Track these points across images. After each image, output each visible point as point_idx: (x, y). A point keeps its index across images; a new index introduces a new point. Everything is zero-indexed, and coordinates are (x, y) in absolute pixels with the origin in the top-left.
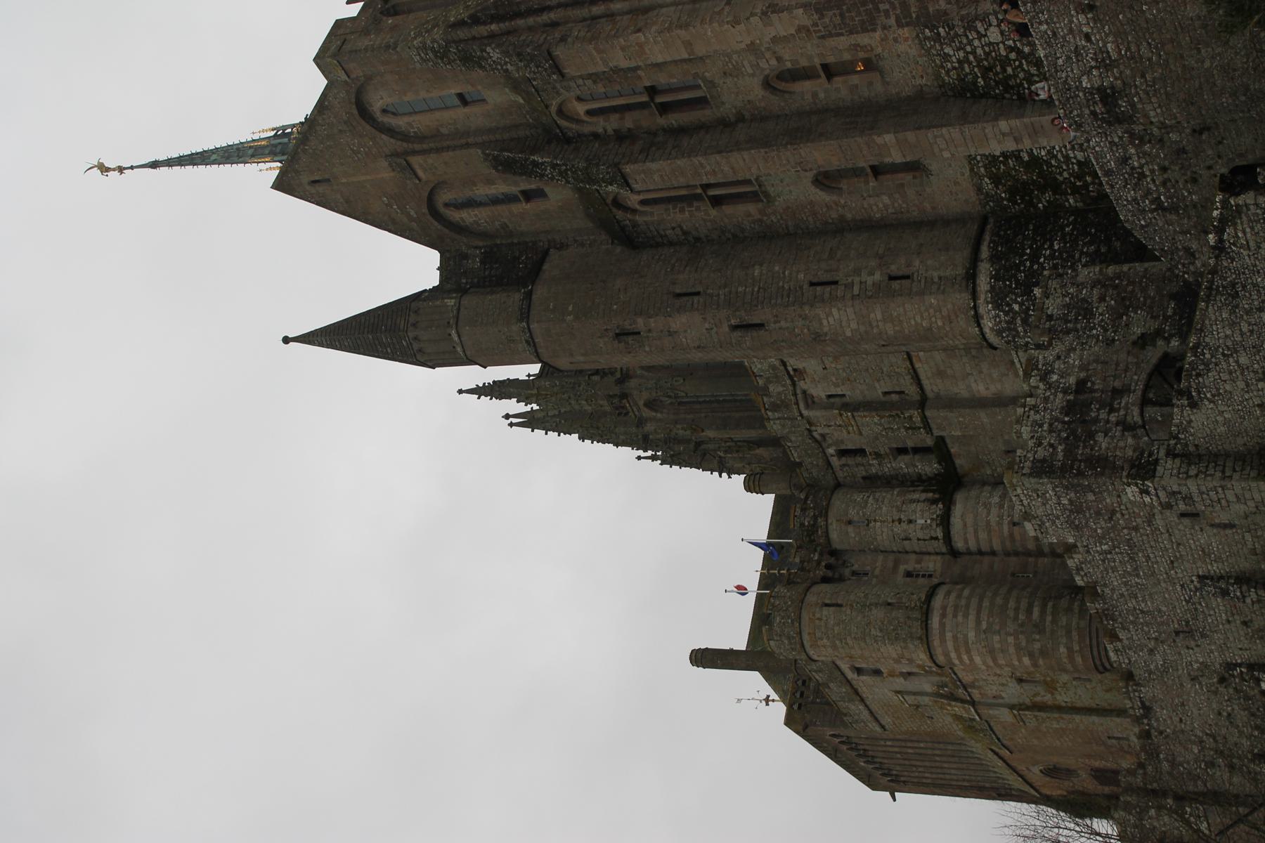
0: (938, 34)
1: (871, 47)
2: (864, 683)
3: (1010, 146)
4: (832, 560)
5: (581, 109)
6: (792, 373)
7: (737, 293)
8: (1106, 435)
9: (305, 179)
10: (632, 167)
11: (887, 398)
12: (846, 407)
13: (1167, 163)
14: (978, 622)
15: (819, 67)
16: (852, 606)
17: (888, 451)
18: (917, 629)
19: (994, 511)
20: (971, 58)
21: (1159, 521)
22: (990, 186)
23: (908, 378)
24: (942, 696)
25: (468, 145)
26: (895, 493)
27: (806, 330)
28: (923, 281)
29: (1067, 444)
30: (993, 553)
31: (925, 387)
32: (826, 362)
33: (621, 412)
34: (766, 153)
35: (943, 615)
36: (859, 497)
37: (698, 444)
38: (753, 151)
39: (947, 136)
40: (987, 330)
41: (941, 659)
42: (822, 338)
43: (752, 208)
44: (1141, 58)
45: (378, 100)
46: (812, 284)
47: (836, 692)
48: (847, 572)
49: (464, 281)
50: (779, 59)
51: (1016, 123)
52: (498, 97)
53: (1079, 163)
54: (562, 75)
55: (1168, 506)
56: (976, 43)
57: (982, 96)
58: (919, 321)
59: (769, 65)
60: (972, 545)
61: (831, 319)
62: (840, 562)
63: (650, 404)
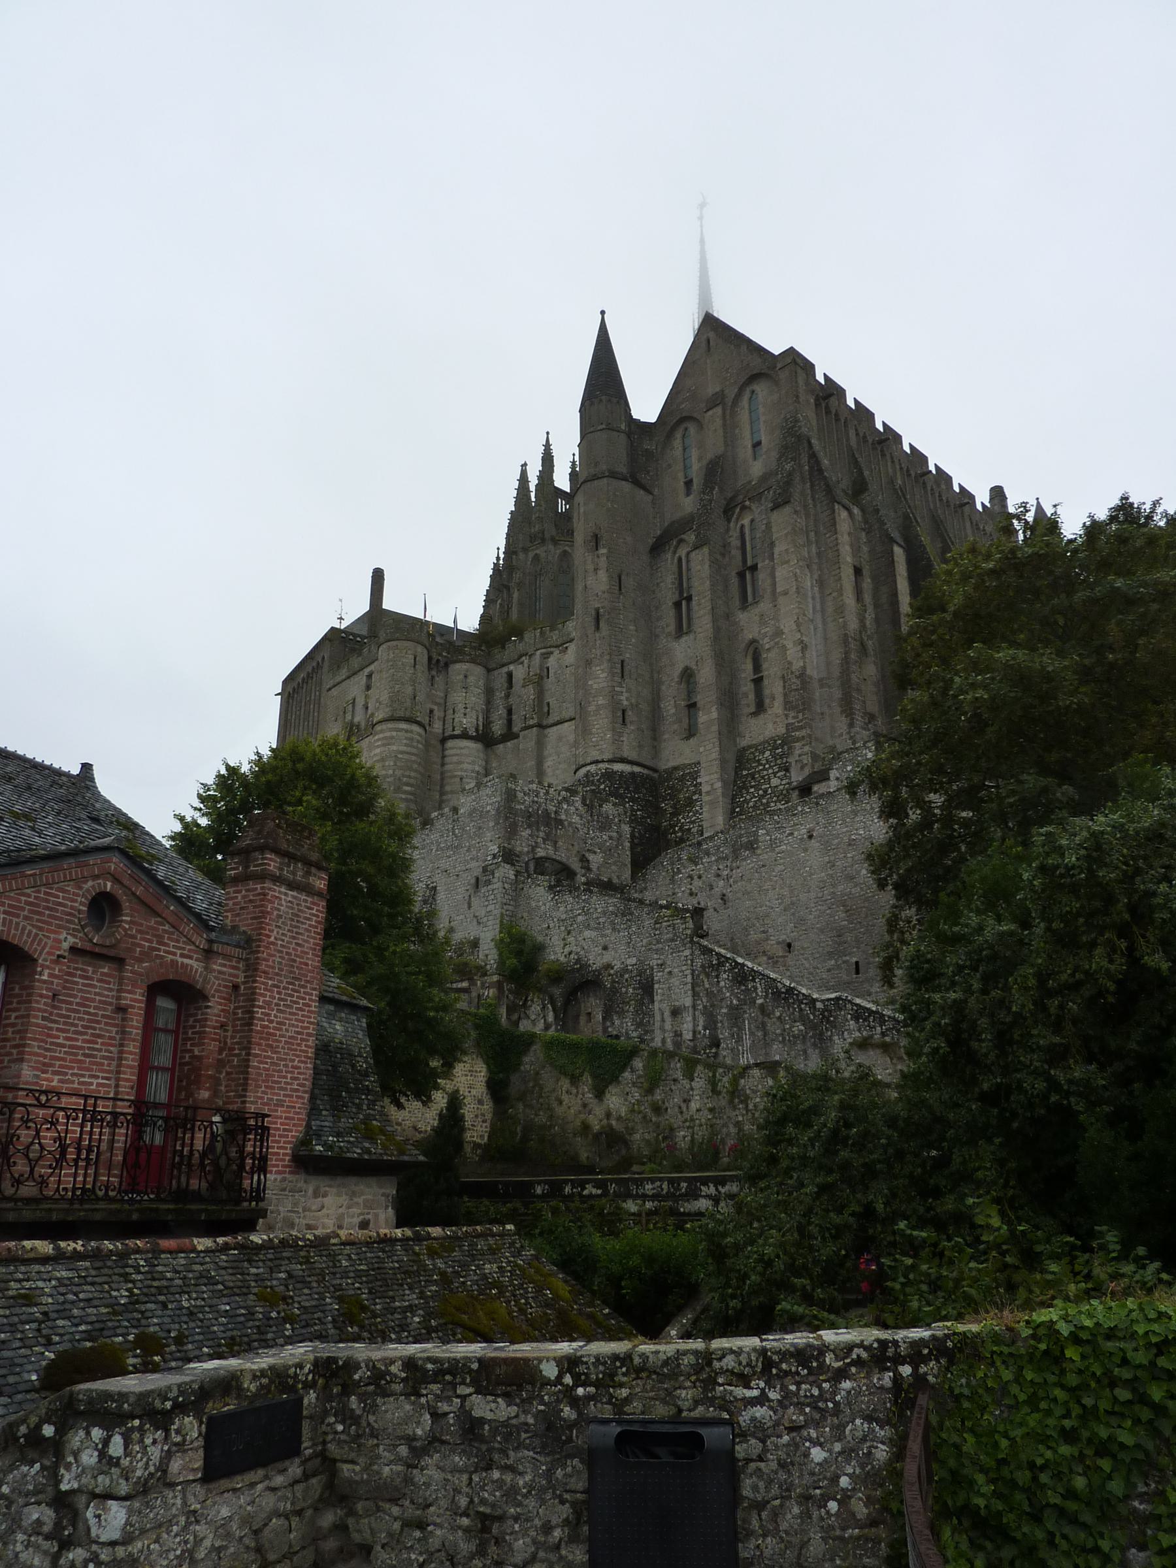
2: (361, 679)
3: (705, 788)
4: (442, 664)
5: (746, 521)
12: (541, 678)
13: (704, 878)
14: (402, 752)
18: (401, 714)
19: (470, 767)
21: (474, 864)
23: (557, 719)
24: (351, 728)
25: (726, 444)
30: (443, 765)
33: (532, 538)
35: (407, 731)
36: (481, 683)
37: (508, 588)
40: (588, 768)
41: (378, 728)
43: (672, 628)
45: (761, 390)
46: (622, 662)
47: (355, 662)
48: (434, 673)
51: (720, 791)
52: (757, 469)
53: (689, 829)
54: (772, 510)
55: (485, 870)
57: (736, 773)
59: (766, 643)
60: (447, 753)
63: (536, 557)
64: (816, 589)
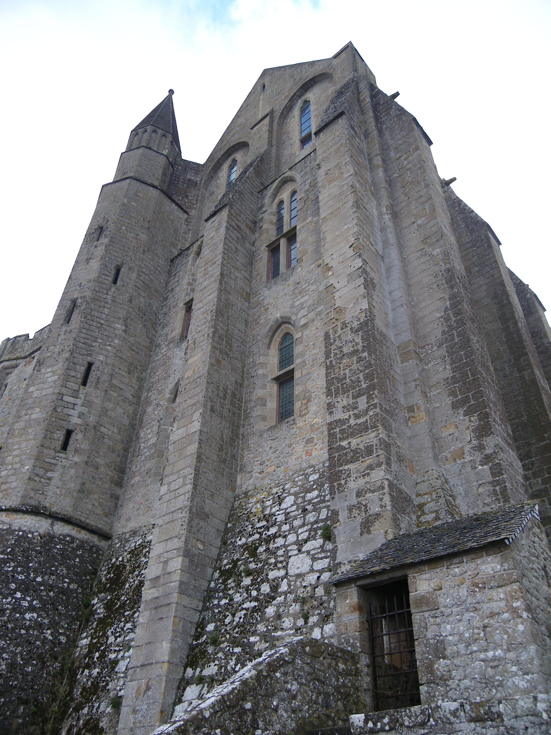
0: (310, 491)
1: (305, 414)
5: (285, 195)
6: (33, 355)
7: (104, 307)
9: (267, 81)
10: (226, 214)
15: (291, 367)
20: (273, 530)
22: (133, 545)
25: (270, 144)
27: (49, 354)
28: (53, 461)
34: (212, 311)
38: (216, 300)
39: (182, 491)
42: (37, 368)
43: (178, 331)
46: (90, 365)
49: (180, 168)
50: (305, 326)
56: (292, 538)
58: (14, 453)
64: (387, 217)
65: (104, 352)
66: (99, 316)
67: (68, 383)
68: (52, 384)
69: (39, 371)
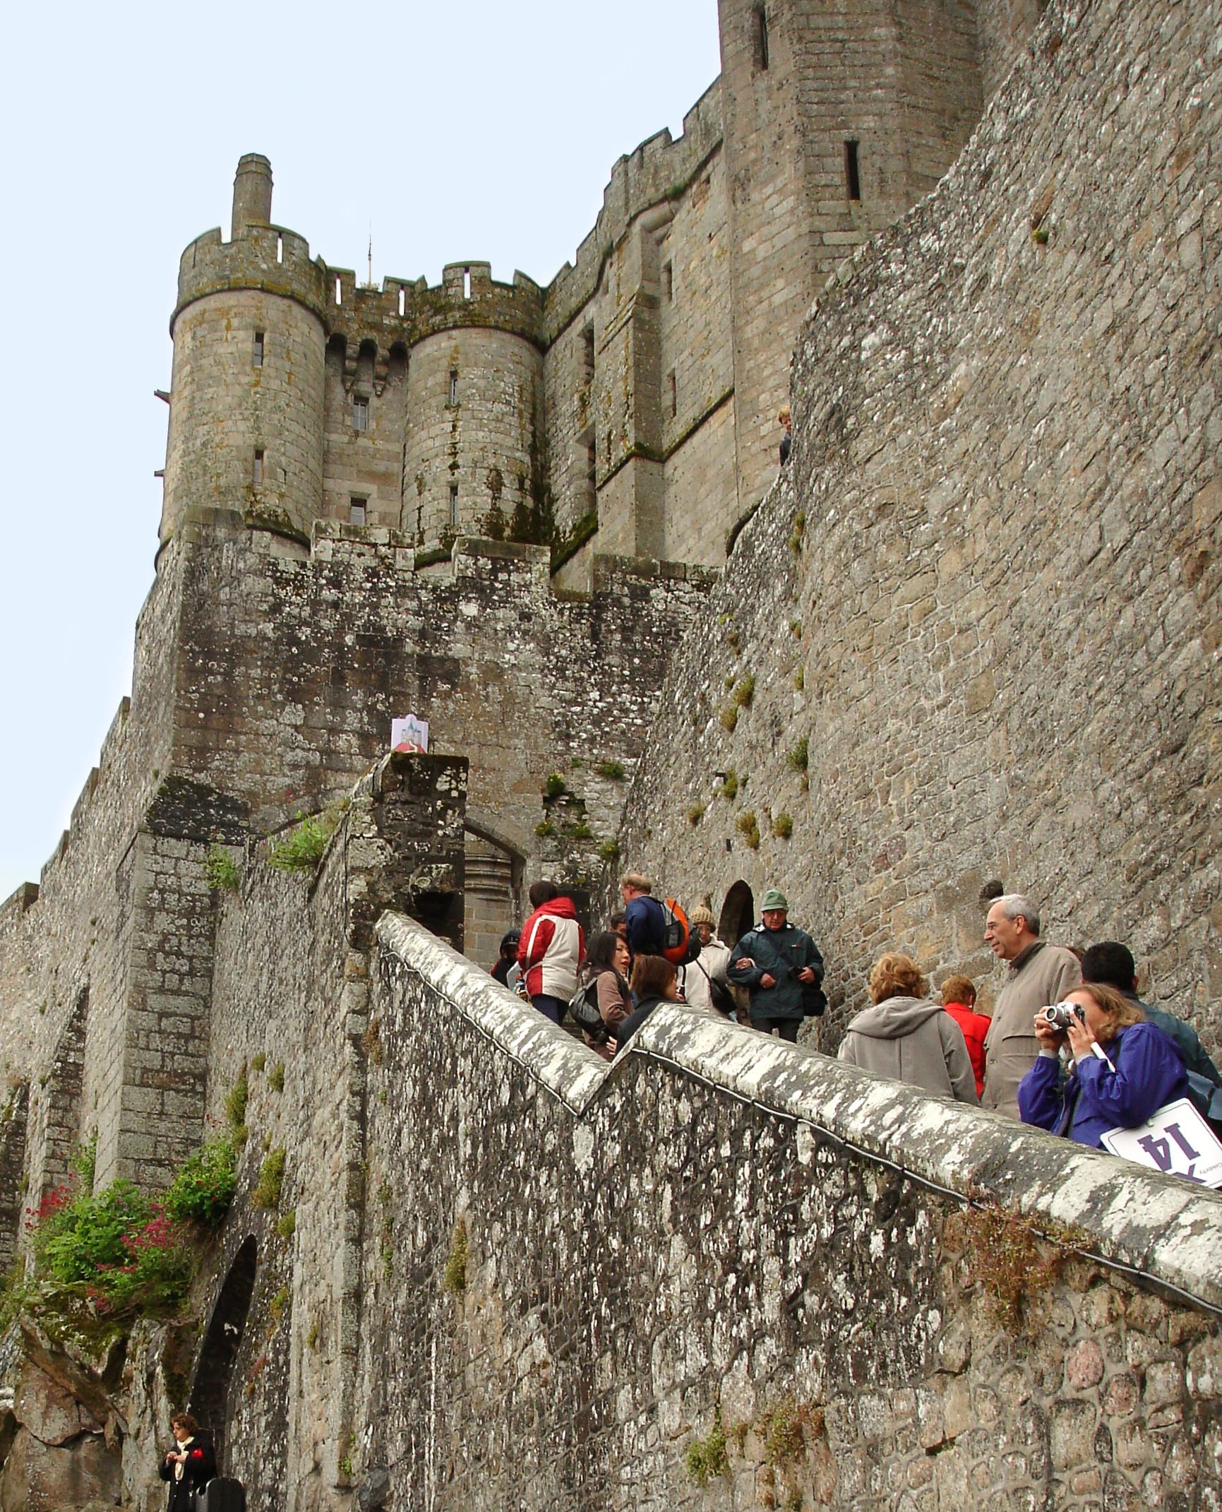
4: (382, 352)
6: (704, 175)
8: (296, 727)
11: (666, 384)
16: (257, 384)
17: (590, 422)
26: (518, 454)
27: (752, 155)
29: (278, 642)
31: (682, 450)
32: (720, 235)
36: (509, 384)
42: (739, 193)
44: (929, 485)
46: (852, 147)
61: (775, 199)
62: (382, 370)
65: (874, 107)
66: (829, 25)
67: (821, 204)
68: (787, 219)
69: (746, 200)
